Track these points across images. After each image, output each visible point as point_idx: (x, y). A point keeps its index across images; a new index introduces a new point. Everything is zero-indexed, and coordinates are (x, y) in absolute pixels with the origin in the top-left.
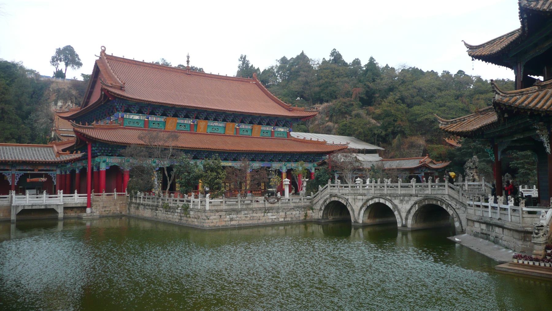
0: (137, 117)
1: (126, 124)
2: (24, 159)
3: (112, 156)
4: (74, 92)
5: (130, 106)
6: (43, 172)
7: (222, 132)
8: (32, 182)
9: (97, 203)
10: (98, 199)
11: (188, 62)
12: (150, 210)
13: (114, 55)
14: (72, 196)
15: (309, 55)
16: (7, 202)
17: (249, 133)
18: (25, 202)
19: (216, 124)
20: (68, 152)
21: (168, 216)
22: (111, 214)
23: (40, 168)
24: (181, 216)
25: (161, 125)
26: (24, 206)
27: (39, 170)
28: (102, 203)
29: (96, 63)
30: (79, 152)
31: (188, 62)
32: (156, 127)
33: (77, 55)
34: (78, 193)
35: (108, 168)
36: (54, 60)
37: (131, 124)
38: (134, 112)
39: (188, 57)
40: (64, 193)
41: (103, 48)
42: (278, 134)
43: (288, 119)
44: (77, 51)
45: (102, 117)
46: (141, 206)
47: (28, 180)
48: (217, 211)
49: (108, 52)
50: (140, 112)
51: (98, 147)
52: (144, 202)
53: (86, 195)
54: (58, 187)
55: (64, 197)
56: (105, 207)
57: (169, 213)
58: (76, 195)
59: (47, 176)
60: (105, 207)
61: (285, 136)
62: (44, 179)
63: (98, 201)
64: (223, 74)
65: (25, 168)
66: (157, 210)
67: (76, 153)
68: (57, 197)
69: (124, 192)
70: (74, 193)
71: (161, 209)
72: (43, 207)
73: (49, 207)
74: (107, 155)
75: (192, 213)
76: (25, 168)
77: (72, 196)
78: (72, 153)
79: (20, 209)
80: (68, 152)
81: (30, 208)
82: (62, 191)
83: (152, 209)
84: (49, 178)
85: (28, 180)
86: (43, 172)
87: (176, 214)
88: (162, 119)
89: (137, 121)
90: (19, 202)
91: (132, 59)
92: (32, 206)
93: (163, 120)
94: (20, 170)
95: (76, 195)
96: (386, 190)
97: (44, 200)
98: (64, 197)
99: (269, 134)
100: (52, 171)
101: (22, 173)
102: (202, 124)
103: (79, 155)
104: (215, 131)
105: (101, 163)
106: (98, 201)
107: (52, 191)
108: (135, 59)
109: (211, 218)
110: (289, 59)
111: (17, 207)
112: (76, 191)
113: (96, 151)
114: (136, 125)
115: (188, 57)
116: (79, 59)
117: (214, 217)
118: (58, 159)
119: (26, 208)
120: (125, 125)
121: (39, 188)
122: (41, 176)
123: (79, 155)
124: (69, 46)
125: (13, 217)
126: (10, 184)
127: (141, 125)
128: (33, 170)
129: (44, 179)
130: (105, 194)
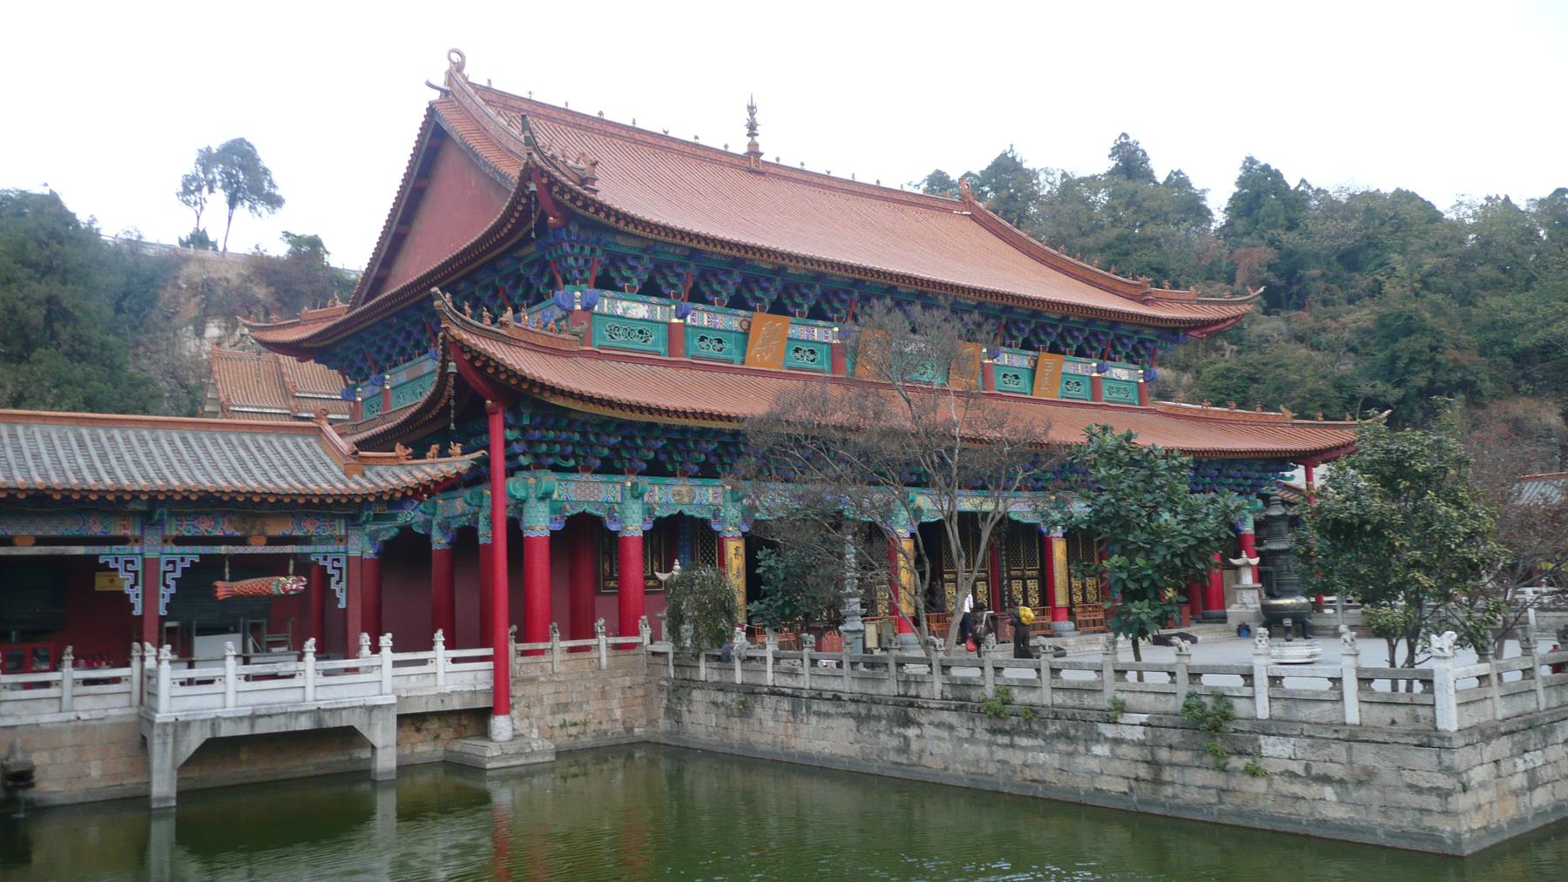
0: (639, 310)
1: (601, 337)
2: (206, 484)
3: (574, 470)
4: (261, 292)
5: (615, 260)
6: (288, 549)
8: (236, 599)
9: (531, 690)
10: (533, 671)
11: (752, 128)
12: (852, 723)
13: (495, 86)
14: (424, 662)
15: (1030, 160)
16: (123, 700)
17: (1024, 382)
18: (217, 700)
20: (400, 450)
21: (1016, 758)
22: (587, 740)
23: (276, 530)
24: (1154, 764)
25: (727, 345)
26: (215, 722)
27: (273, 541)
28: (550, 689)
29: (431, 111)
30: (456, 448)
31: (752, 128)
32: (712, 352)
33: (266, 172)
35: (558, 527)
36: (190, 188)
37: (620, 340)
38: (632, 289)
39: (752, 109)
40: (394, 650)
41: (455, 57)
43: (1148, 334)
44: (266, 158)
45: (389, 357)
46: (770, 701)
47: (223, 589)
49: (476, 73)
50: (650, 289)
51: (524, 430)
52: (786, 682)
53: (489, 651)
54: (355, 620)
55: (396, 664)
56: (563, 707)
57: (1024, 741)
59: (303, 566)
60: (563, 707)
61: (1133, 397)
62: (291, 584)
63: (532, 680)
65: (205, 528)
66: (908, 722)
67: (443, 453)
68: (355, 670)
69: (636, 633)
71: (947, 717)
72: (304, 724)
73: (331, 722)
74: (555, 468)
75: (1275, 749)
76: (205, 528)
77: (424, 662)
78: (419, 453)
79: (194, 741)
80: (400, 450)
81: (244, 730)
82: (386, 640)
83: (857, 718)
84: (318, 577)
85: (223, 589)
86: (288, 549)
87: (1099, 749)
88: (731, 321)
89: (642, 328)
90: (191, 703)
91: (562, 105)
92: (254, 718)
93: (734, 324)
94: (180, 541)
97: (307, 687)
98: (396, 664)
99: (1085, 388)
101: (193, 553)
103: (458, 462)
105: (532, 501)
106: (532, 680)
108: (572, 107)
110: (955, 176)
111: (181, 727)
112: (439, 637)
113: (517, 448)
114: (636, 343)
115: (752, 109)
116: (271, 184)
118: (358, 484)
119: (226, 731)
120: (598, 342)
121: (271, 628)
122: (274, 566)
123: (458, 462)
124: (242, 141)
125: (163, 786)
126: (137, 611)
127: (657, 342)
128: (242, 541)
129: (291, 584)
130: (560, 644)
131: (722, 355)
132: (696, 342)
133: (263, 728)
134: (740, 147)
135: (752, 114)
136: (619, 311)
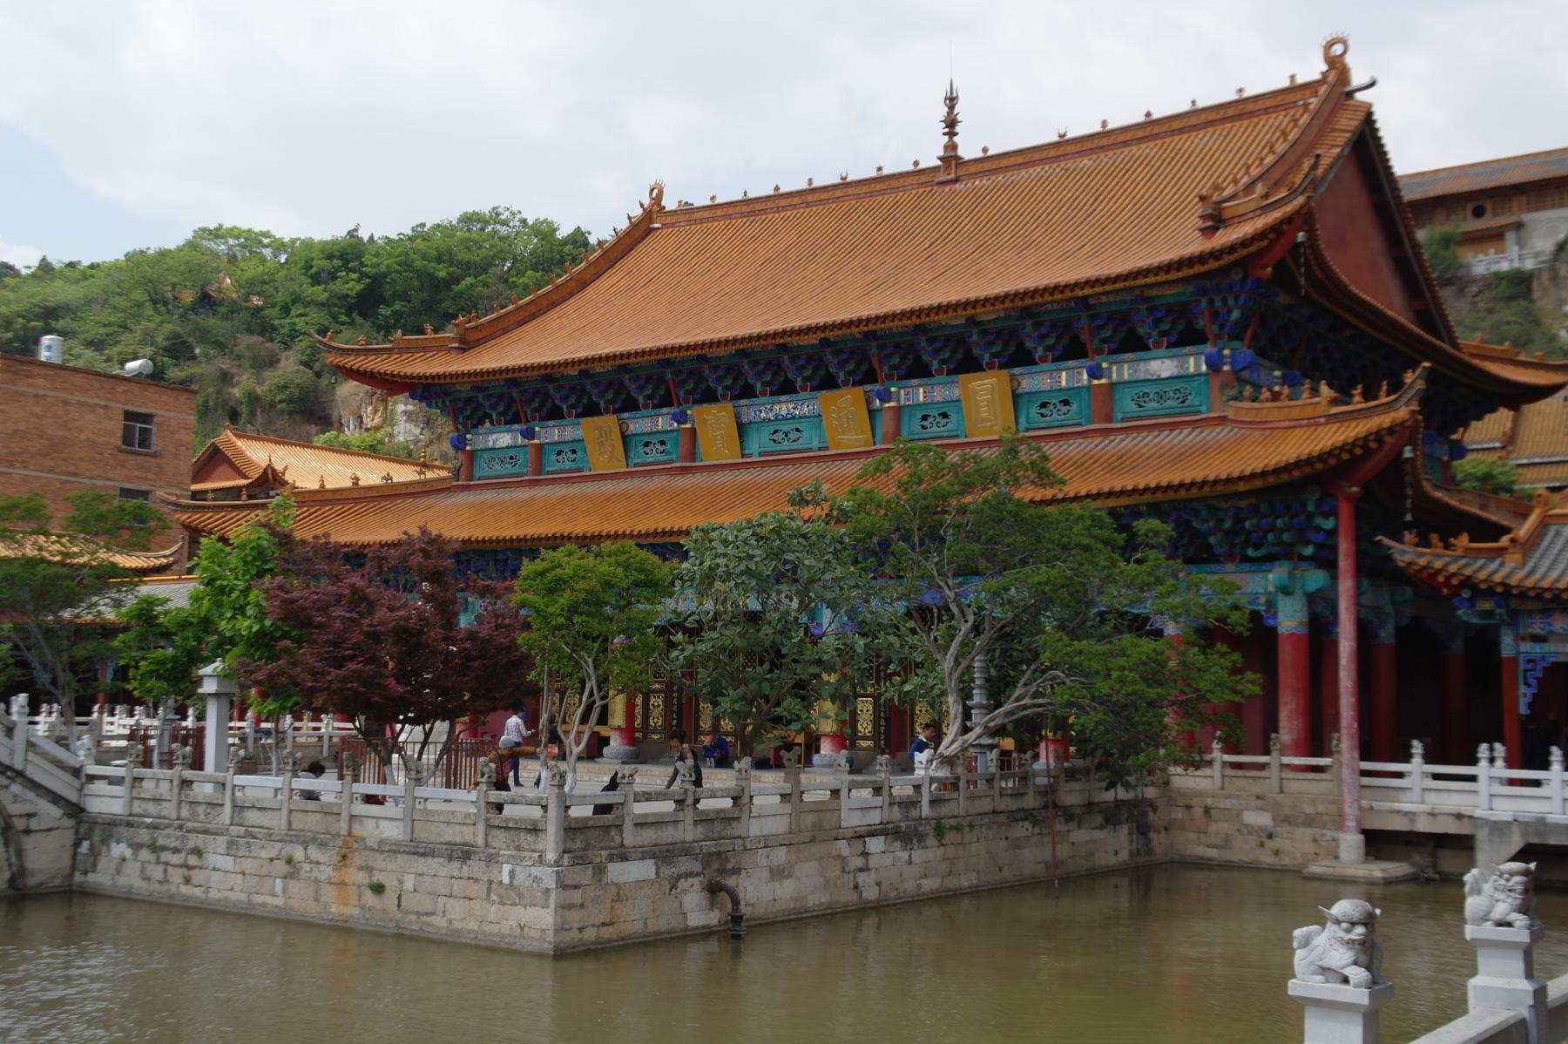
1: (482, 469)
7: (815, 444)
11: (951, 124)
19: (784, 407)
31: (951, 124)
32: (568, 465)
37: (498, 469)
39: (951, 101)
42: (1140, 399)
49: (670, 204)
64: (1125, 115)
89: (510, 454)
96: (1483, 799)
102: (714, 421)
104: (786, 445)
108: (751, 195)
114: (509, 469)
115: (951, 101)
131: (574, 466)
132: (554, 458)
134: (930, 157)
135: (951, 108)
136: (490, 444)
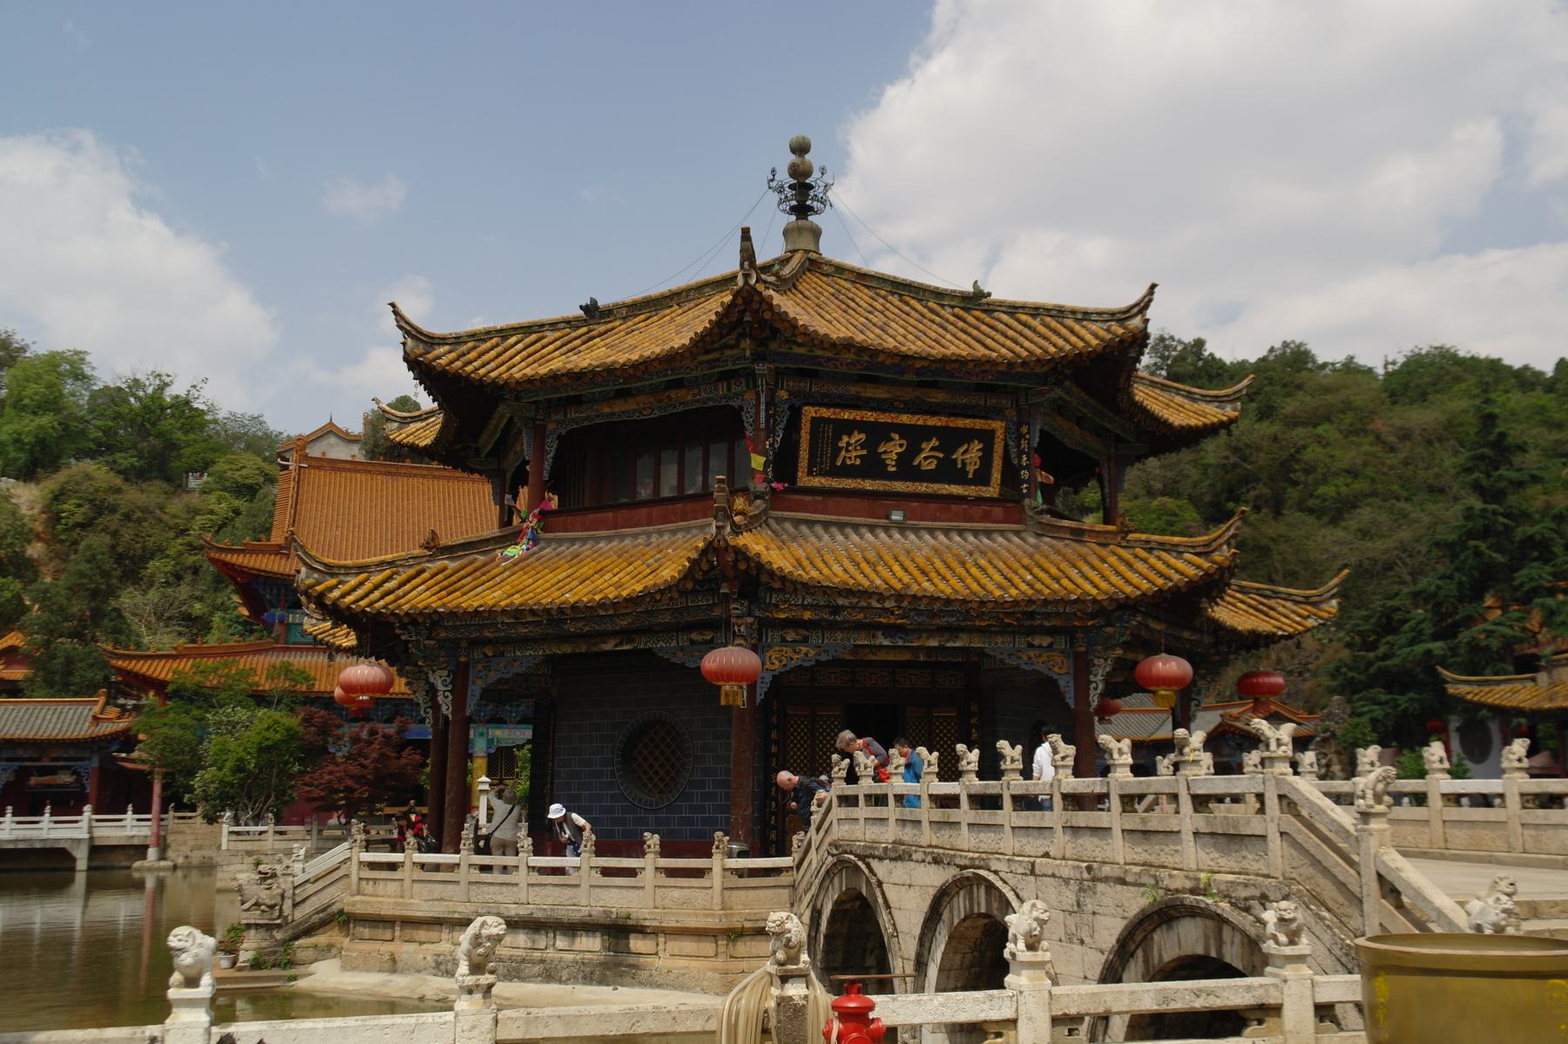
1: (295, 636)
9: (180, 837)
27: (53, 760)
34: (135, 812)
48: (249, 853)
58: (129, 816)
65: (20, 753)
70: (125, 812)
92: (17, 841)
94: (8, 760)
95: (129, 816)
100: (82, 759)
106: (181, 832)
107: (67, 805)
109: (232, 868)
117: (240, 867)
128: (38, 760)
133: (21, 846)
